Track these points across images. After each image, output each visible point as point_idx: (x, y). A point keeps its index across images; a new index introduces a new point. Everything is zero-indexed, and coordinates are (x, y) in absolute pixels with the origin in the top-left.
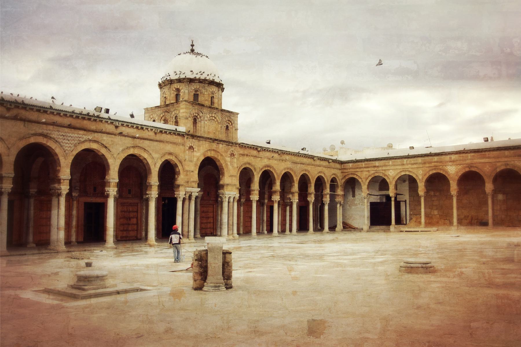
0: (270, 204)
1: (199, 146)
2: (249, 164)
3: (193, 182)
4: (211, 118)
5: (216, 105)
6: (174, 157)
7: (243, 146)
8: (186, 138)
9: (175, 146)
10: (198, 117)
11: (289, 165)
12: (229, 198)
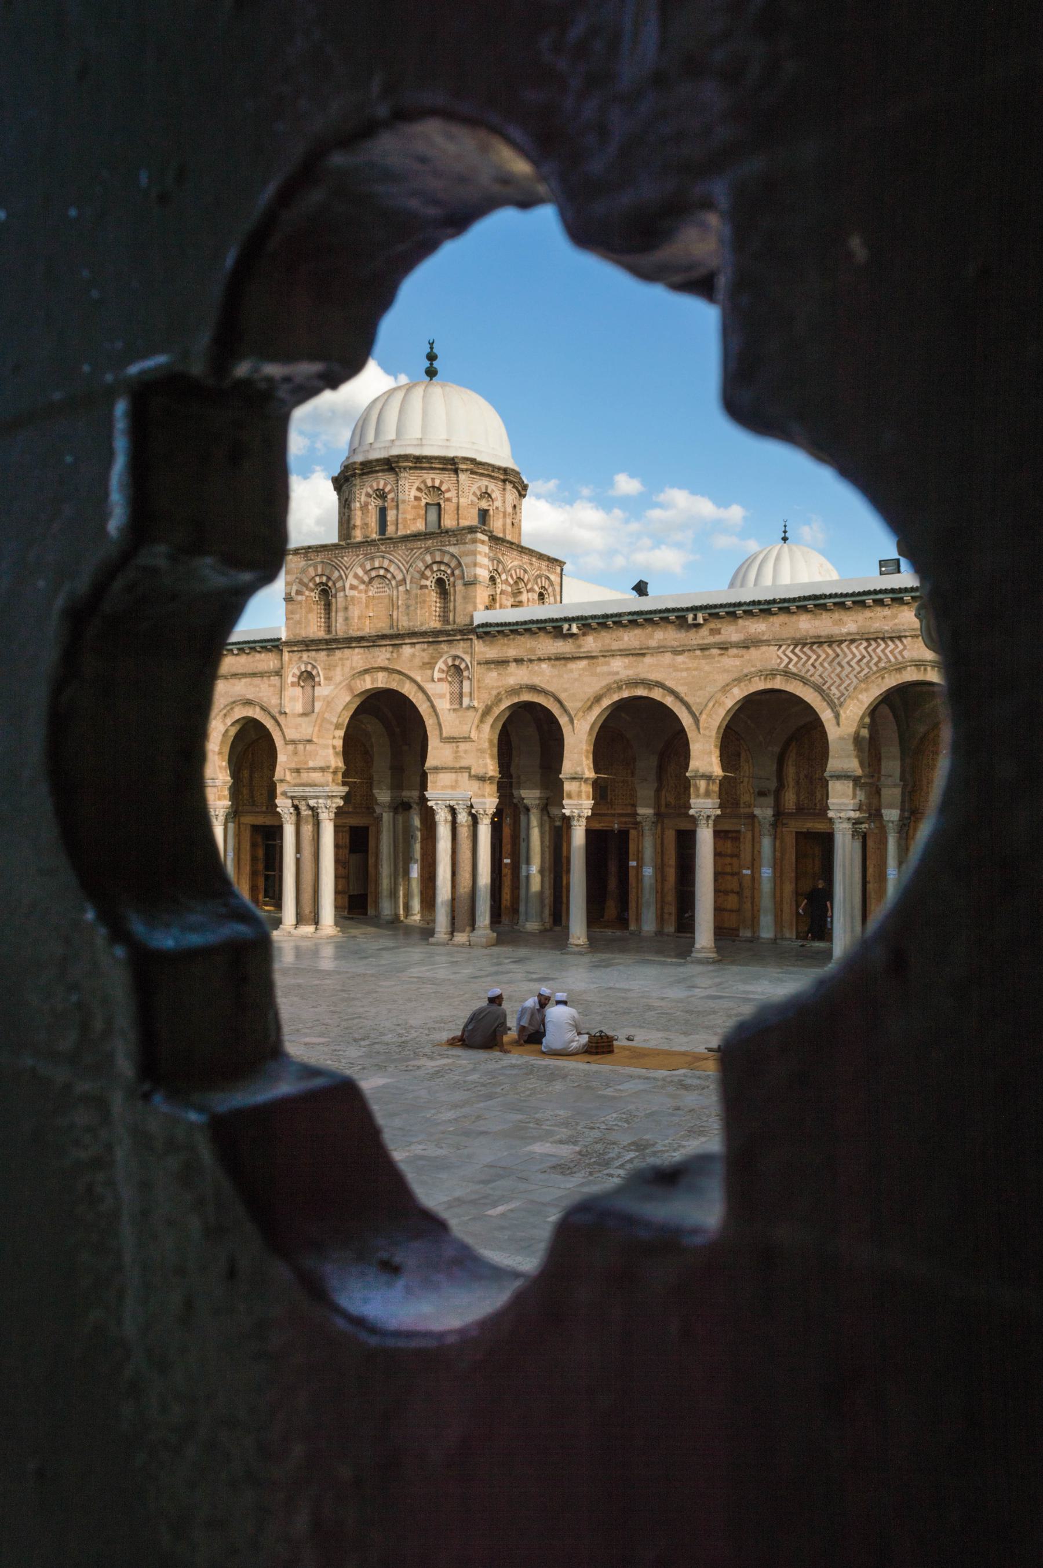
0: (685, 826)
1: (329, 668)
2: (533, 689)
3: (314, 769)
4: (373, 574)
5: (390, 529)
6: (258, 709)
7: (488, 632)
8: (286, 656)
9: (257, 681)
10: (330, 584)
11: (772, 657)
12: (453, 811)
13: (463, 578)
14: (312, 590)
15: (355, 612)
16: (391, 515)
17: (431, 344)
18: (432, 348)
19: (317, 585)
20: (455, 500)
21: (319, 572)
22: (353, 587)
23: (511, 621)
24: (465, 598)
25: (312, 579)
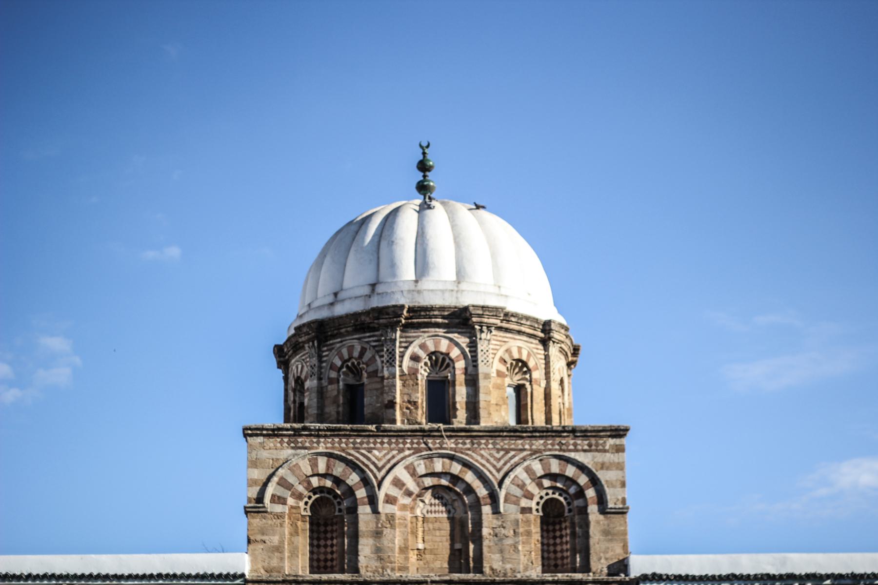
4: (429, 482)
13: (601, 500)
14: (299, 497)
15: (395, 538)
16: (461, 393)
17: (424, 149)
18: (424, 153)
19: (314, 491)
20: (543, 384)
21: (322, 467)
22: (390, 500)
23: (691, 572)
24: (606, 533)
25: (306, 480)
